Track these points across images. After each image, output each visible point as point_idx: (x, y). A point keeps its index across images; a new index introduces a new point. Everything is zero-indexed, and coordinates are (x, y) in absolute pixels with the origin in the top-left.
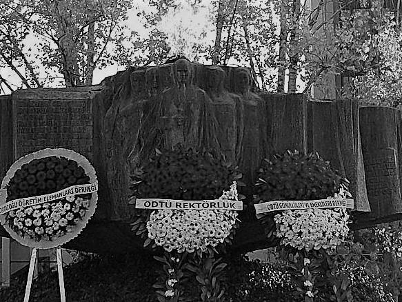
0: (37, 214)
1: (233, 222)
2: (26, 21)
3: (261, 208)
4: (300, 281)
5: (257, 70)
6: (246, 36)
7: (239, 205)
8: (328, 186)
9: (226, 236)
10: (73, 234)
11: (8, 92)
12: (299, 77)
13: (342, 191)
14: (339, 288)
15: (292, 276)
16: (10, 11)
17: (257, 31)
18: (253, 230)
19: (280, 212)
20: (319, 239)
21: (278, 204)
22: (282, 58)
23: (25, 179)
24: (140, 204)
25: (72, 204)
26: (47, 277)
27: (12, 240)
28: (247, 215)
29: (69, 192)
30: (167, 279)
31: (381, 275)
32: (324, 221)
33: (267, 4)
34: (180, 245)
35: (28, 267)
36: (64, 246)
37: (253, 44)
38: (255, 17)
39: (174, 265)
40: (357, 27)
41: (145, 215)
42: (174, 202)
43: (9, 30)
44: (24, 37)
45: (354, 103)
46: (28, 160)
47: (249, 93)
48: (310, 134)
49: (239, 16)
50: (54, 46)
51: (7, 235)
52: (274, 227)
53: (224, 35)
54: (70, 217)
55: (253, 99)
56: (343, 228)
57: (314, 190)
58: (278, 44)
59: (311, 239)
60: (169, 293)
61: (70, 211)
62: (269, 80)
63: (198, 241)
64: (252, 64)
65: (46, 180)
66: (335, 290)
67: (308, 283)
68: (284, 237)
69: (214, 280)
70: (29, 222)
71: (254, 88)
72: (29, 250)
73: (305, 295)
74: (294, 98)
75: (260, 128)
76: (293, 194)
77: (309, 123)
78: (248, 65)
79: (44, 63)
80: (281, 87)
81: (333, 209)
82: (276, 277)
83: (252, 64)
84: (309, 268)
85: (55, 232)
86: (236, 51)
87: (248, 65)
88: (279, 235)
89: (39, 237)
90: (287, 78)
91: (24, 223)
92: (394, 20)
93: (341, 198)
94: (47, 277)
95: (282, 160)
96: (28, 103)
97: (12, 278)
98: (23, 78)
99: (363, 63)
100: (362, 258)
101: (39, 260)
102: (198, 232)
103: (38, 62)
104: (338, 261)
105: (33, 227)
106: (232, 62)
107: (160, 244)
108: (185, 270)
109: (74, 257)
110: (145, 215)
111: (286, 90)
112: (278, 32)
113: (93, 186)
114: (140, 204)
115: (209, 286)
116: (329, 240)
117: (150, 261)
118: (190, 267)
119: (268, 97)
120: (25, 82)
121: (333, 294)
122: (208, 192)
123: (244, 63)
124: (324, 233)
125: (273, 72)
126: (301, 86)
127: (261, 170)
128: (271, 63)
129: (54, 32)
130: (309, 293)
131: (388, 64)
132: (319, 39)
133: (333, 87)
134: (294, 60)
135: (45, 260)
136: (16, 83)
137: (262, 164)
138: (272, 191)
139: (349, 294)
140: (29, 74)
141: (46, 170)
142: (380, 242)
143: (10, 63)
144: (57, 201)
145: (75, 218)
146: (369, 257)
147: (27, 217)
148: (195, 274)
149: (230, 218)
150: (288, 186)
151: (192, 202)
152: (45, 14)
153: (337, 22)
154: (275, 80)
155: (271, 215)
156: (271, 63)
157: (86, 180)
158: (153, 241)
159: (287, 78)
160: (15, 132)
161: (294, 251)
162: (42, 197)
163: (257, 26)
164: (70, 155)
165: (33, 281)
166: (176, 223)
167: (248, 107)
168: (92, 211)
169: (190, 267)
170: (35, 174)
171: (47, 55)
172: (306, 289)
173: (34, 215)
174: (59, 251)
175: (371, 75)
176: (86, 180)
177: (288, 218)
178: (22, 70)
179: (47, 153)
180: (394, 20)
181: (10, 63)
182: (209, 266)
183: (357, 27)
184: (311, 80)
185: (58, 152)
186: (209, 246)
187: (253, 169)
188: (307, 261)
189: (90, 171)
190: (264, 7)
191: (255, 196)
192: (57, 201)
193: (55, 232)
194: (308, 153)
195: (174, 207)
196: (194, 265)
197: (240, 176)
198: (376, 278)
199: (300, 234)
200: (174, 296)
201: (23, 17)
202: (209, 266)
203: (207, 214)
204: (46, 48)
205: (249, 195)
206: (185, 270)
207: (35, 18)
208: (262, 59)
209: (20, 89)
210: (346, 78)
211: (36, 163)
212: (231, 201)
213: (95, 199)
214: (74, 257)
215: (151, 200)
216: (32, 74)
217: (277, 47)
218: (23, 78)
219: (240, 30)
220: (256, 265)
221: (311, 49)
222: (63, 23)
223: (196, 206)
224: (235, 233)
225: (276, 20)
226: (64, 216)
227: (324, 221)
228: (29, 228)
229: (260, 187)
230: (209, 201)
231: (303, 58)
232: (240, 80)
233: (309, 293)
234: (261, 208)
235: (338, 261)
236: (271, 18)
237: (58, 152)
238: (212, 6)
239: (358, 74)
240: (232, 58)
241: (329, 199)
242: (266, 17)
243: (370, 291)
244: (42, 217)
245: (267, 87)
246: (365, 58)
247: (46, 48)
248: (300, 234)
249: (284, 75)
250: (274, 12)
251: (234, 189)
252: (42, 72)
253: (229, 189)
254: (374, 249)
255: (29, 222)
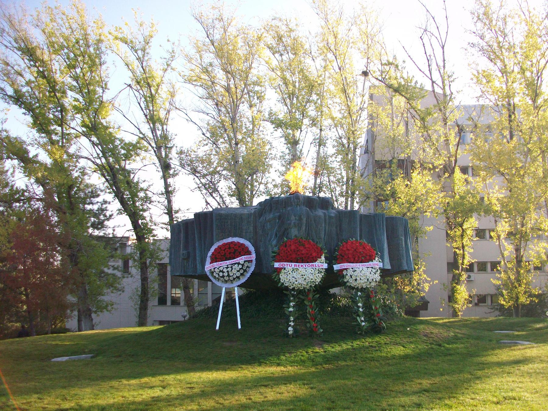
0: (225, 270)
1: (323, 274)
2: (220, 174)
3: (336, 267)
4: (355, 303)
5: (334, 198)
6: (329, 182)
7: (325, 266)
8: (370, 256)
9: (319, 281)
10: (243, 280)
11: (211, 210)
12: (355, 202)
13: (377, 259)
14: (375, 307)
15: (352, 301)
16: (212, 169)
17: (335, 179)
18: (332, 278)
19: (346, 269)
20: (365, 282)
21: (345, 265)
22: (347, 192)
23: (219, 253)
24: (277, 265)
25: (243, 265)
26: (230, 301)
27: (213, 283)
28: (330, 270)
29: (241, 259)
30: (290, 302)
31: (396, 300)
32: (368, 274)
33: (339, 166)
34: (296, 285)
35: (221, 296)
36: (238, 286)
37: (333, 186)
38: (333, 172)
39: (293, 296)
40: (384, 177)
41: (279, 270)
42: (293, 264)
43: (212, 178)
44: (219, 182)
45: (383, 215)
46: (220, 243)
47: (331, 210)
48: (361, 230)
49: (325, 171)
50: (234, 187)
51: (210, 280)
52: (343, 277)
53: (318, 181)
54: (242, 271)
55: (333, 213)
56: (377, 277)
57: (363, 258)
58: (345, 186)
59: (361, 283)
60: (291, 309)
61: (242, 268)
62: (340, 204)
63: (305, 283)
64: (332, 195)
65: (230, 253)
66: (373, 308)
67: (360, 304)
68: (348, 281)
69: (313, 303)
70: (221, 274)
71: (333, 208)
72: (221, 288)
73: (358, 310)
74: (353, 213)
75: (336, 227)
76: (352, 260)
77: (360, 225)
78: (330, 196)
79: (229, 195)
80: (346, 207)
81: (372, 268)
82: (344, 302)
83: (332, 195)
84: (360, 297)
85: (234, 279)
86: (324, 189)
87: (330, 196)
88: (345, 280)
89: (226, 282)
90: (349, 203)
91: (219, 274)
92: (403, 173)
93: (377, 263)
94: (230, 301)
95: (347, 243)
96: (220, 215)
97: (213, 302)
98: (218, 203)
99: (387, 195)
100: (387, 292)
101: (227, 293)
102: (305, 279)
103: (226, 195)
104: (375, 293)
105: (223, 276)
106: (322, 195)
107: (286, 285)
108: (299, 298)
109: (243, 291)
110: (279, 270)
111: (349, 208)
112: (345, 180)
113: (253, 256)
114: (277, 265)
115: (311, 306)
116: (370, 283)
117: (281, 293)
118: (301, 297)
119: (340, 212)
120: (219, 204)
121: (372, 309)
122: (310, 259)
123: (328, 195)
124: (368, 279)
125: (343, 199)
126: (356, 207)
127: (337, 248)
128: (341, 195)
129: (233, 180)
130: (361, 310)
131: (399, 195)
132: (366, 183)
133: (372, 207)
134: (353, 194)
135: (229, 293)
136: (215, 205)
137: (337, 245)
138: (342, 259)
139: (380, 310)
140: (221, 200)
141: (230, 248)
142: (396, 284)
143: (212, 195)
144: (235, 264)
145: (244, 272)
146: (390, 292)
147: (220, 271)
148: (304, 300)
149: (321, 272)
150: (350, 256)
151: (302, 264)
152: (229, 170)
153: (374, 175)
154: (344, 203)
155: (341, 271)
156: (341, 195)
157: (249, 253)
158: (283, 284)
159: (349, 203)
160: (214, 229)
161: (353, 288)
162: (228, 261)
163: (334, 177)
164: (242, 241)
165: (224, 303)
166: (294, 275)
167: (330, 217)
168: (252, 269)
169: (301, 297)
170: (224, 250)
171: (230, 191)
172: (359, 307)
173: (224, 271)
174: (236, 288)
175: (391, 201)
176: (249, 253)
177: (350, 272)
178: (218, 198)
179: (230, 240)
180: (403, 173)
181: (212, 195)
182: (311, 296)
183: (384, 177)
184: (361, 203)
185: (236, 239)
186: (311, 286)
187: (332, 248)
188: (359, 293)
189: (252, 248)
190: (338, 167)
191: (333, 261)
192: (235, 264)
193: (234, 279)
194: (360, 239)
195: (293, 266)
196: (303, 295)
197: (326, 251)
198: (394, 302)
199: (356, 280)
200: (294, 311)
201: (218, 172)
202: (311, 296)
203: (309, 270)
204: (230, 188)
205: (330, 261)
206: (299, 298)
207: (224, 172)
208: (337, 193)
209: (217, 209)
210: (379, 203)
211: (224, 245)
212: (322, 264)
213: (254, 262)
214: (243, 291)
215: (282, 263)
216: (223, 201)
217: (344, 187)
218: (218, 203)
219: (326, 179)
220: (334, 295)
221: (361, 188)
222: (239, 175)
223: (304, 266)
224: (324, 280)
225: (344, 174)
226: (238, 271)
227: (368, 274)
228: (221, 277)
229: (336, 257)
230: (311, 264)
231: (357, 193)
232: (326, 203)
233: (361, 310)
234: (336, 267)
235: (375, 293)
236: (341, 173)
237: (236, 239)
238: (312, 167)
239: (385, 200)
240: (322, 193)
241: (370, 263)
242: (339, 172)
243: (391, 308)
244: (228, 272)
245: (340, 207)
246: (388, 192)
247: (230, 188)
248: (356, 280)
249: (348, 201)
250: (343, 170)
251: (323, 258)
252: (228, 200)
253: (320, 258)
254: (393, 288)
255: (221, 274)
